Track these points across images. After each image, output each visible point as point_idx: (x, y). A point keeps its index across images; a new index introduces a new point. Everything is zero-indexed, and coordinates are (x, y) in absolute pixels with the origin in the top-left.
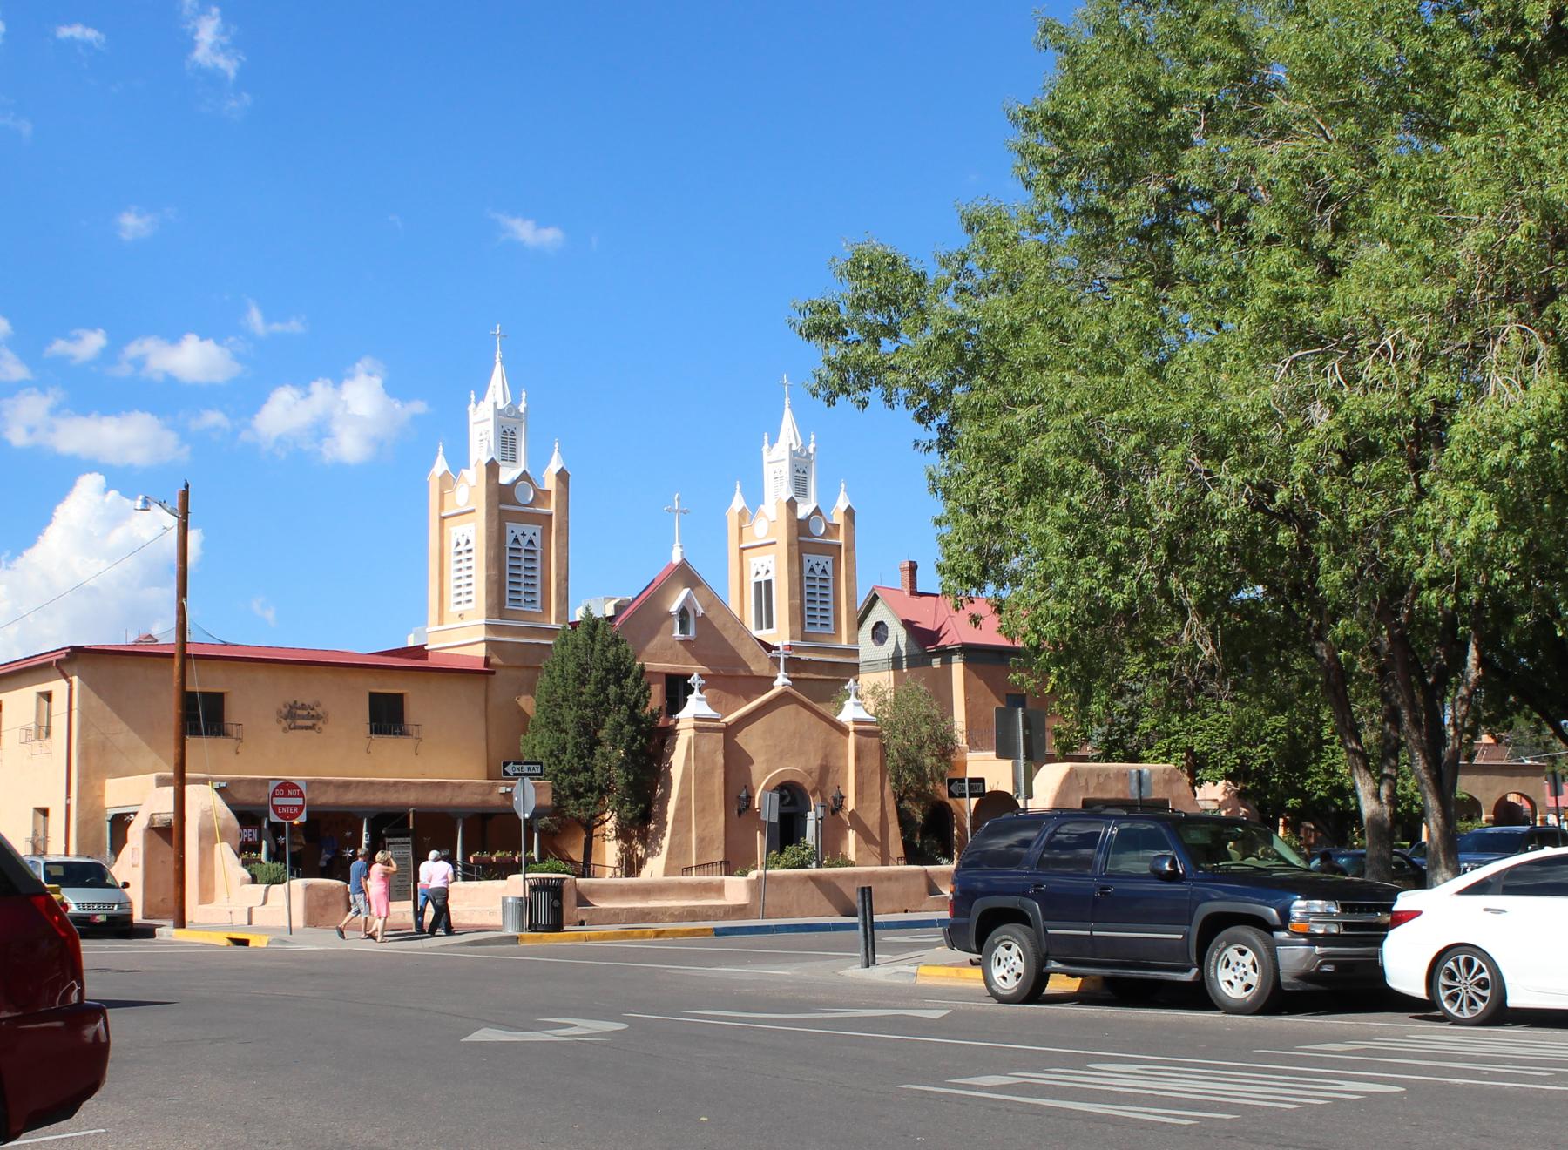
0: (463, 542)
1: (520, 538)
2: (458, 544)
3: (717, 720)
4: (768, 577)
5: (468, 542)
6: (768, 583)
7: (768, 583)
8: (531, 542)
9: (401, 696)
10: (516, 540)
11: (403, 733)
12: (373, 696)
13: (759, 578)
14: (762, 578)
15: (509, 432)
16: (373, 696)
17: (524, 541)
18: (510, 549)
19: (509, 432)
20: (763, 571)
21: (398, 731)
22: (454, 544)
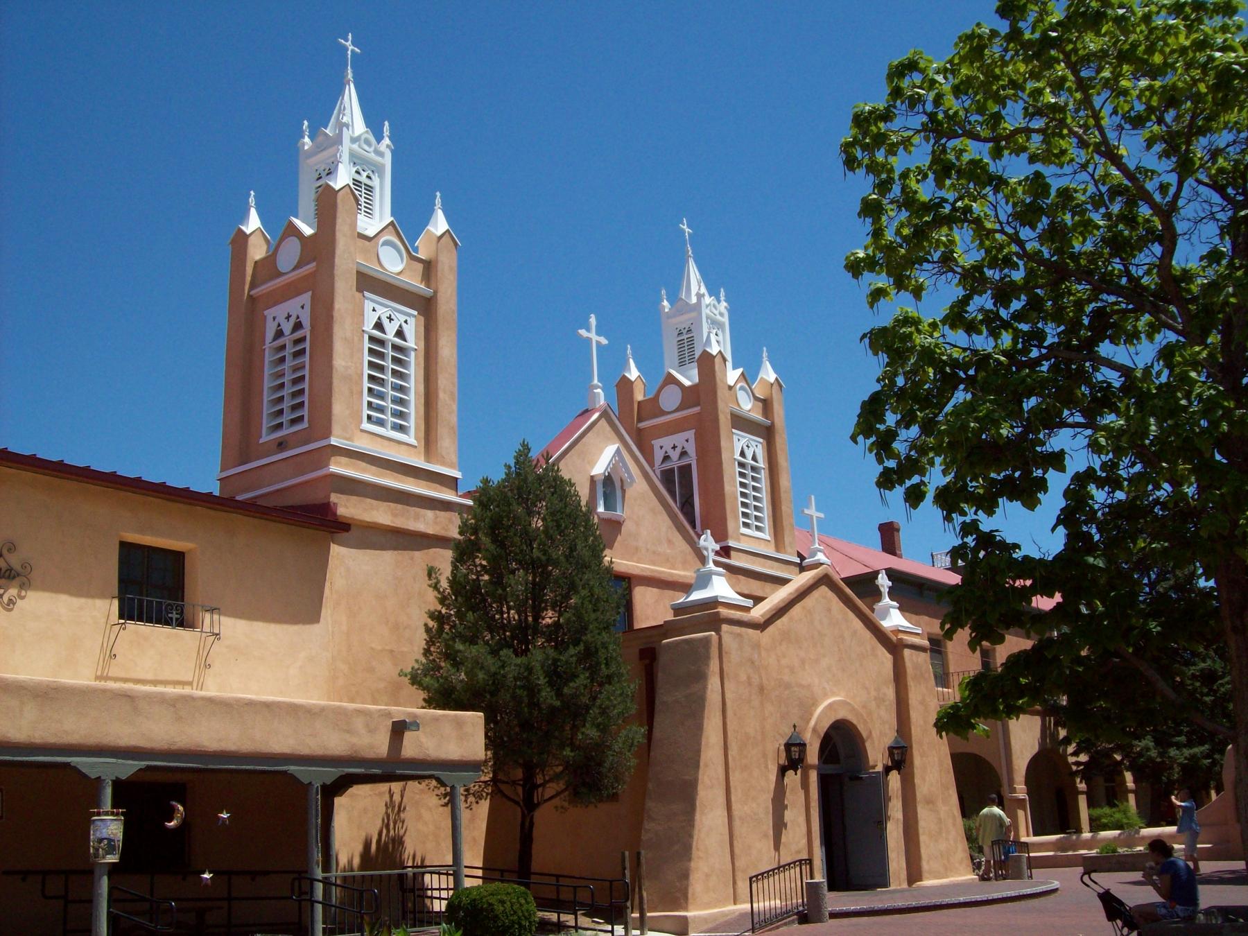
0: (287, 327)
1: (385, 322)
2: (279, 334)
3: (747, 609)
4: (684, 462)
5: (298, 326)
6: (685, 470)
7: (685, 470)
8: (400, 334)
9: (178, 558)
10: (379, 326)
11: (183, 623)
12: (128, 550)
13: (668, 465)
14: (675, 463)
16: (128, 550)
17: (391, 329)
18: (372, 339)
20: (675, 455)
21: (174, 616)
22: (270, 334)
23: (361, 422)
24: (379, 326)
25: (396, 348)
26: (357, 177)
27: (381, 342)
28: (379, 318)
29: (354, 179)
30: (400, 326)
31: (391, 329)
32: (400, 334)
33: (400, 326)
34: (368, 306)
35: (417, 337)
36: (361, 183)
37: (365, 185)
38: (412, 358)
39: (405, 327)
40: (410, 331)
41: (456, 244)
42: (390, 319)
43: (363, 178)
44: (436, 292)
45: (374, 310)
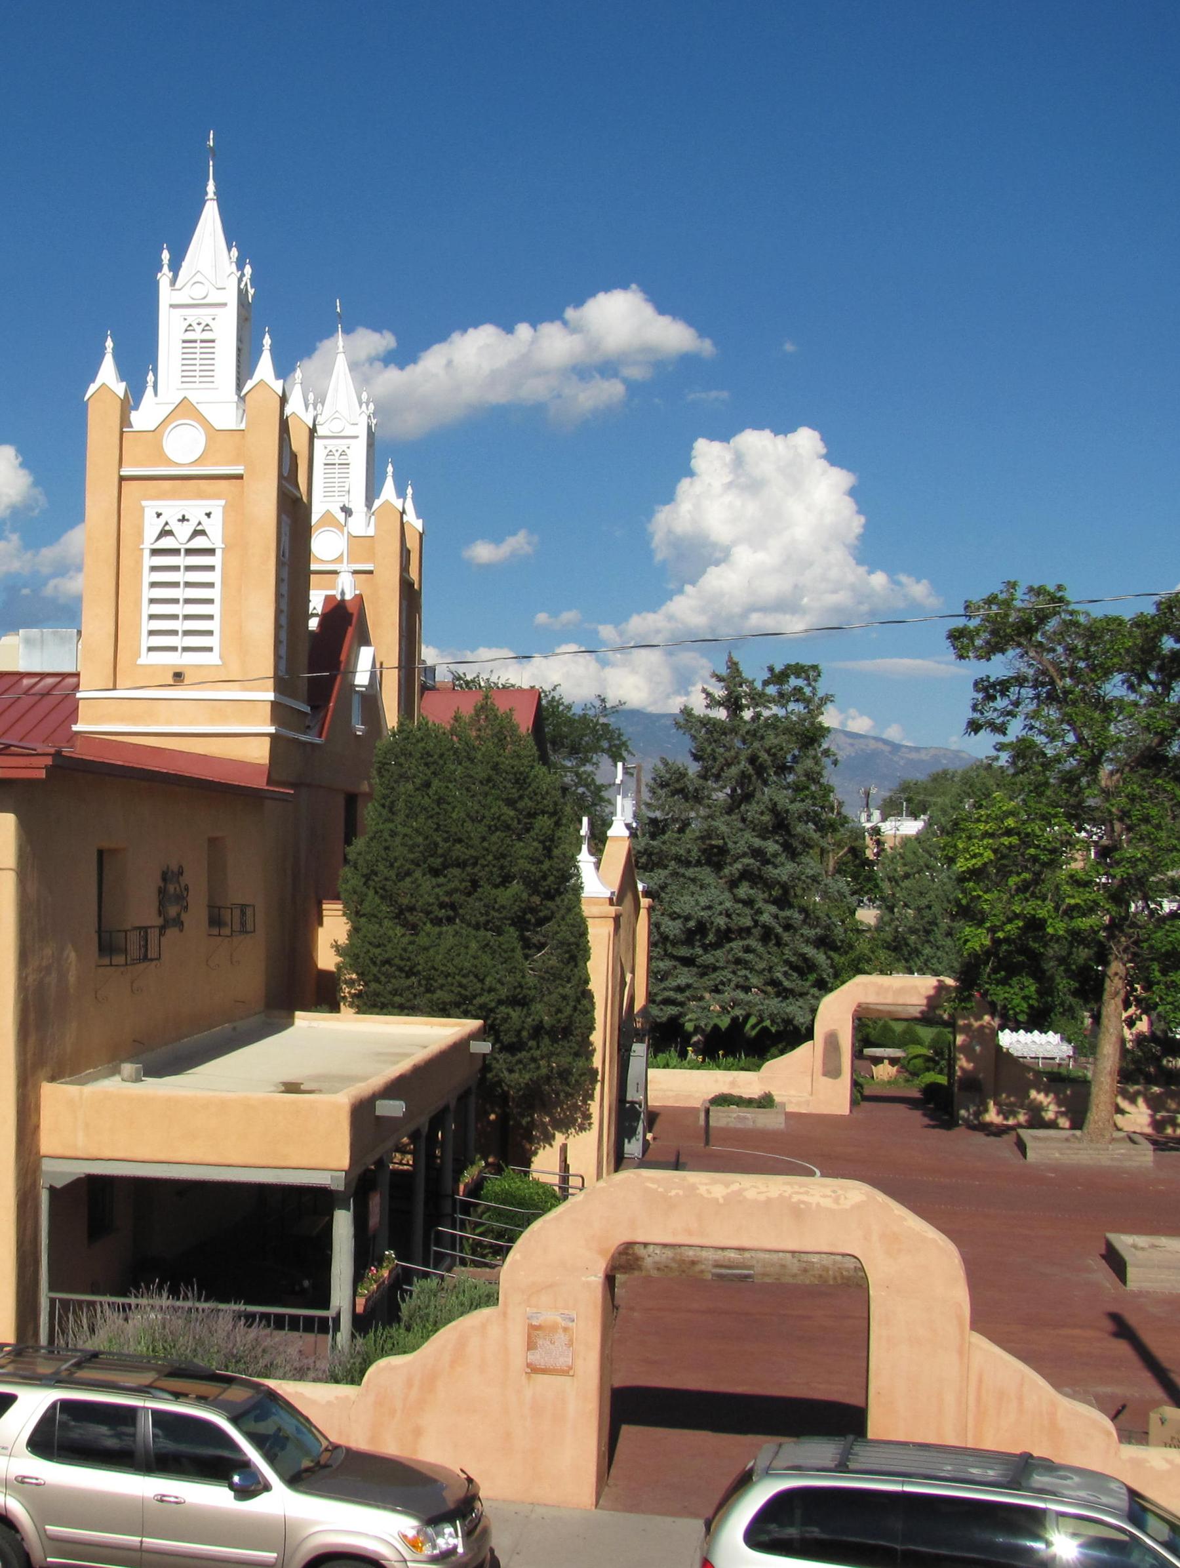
1: (174, 526)
8: (198, 533)
10: (165, 533)
18: (155, 552)
25: (189, 552)
26: (190, 336)
27: (175, 552)
28: (167, 524)
29: (184, 342)
31: (183, 532)
33: (200, 523)
34: (149, 514)
36: (195, 341)
37: (202, 341)
39: (207, 525)
43: (197, 335)
45: (159, 515)
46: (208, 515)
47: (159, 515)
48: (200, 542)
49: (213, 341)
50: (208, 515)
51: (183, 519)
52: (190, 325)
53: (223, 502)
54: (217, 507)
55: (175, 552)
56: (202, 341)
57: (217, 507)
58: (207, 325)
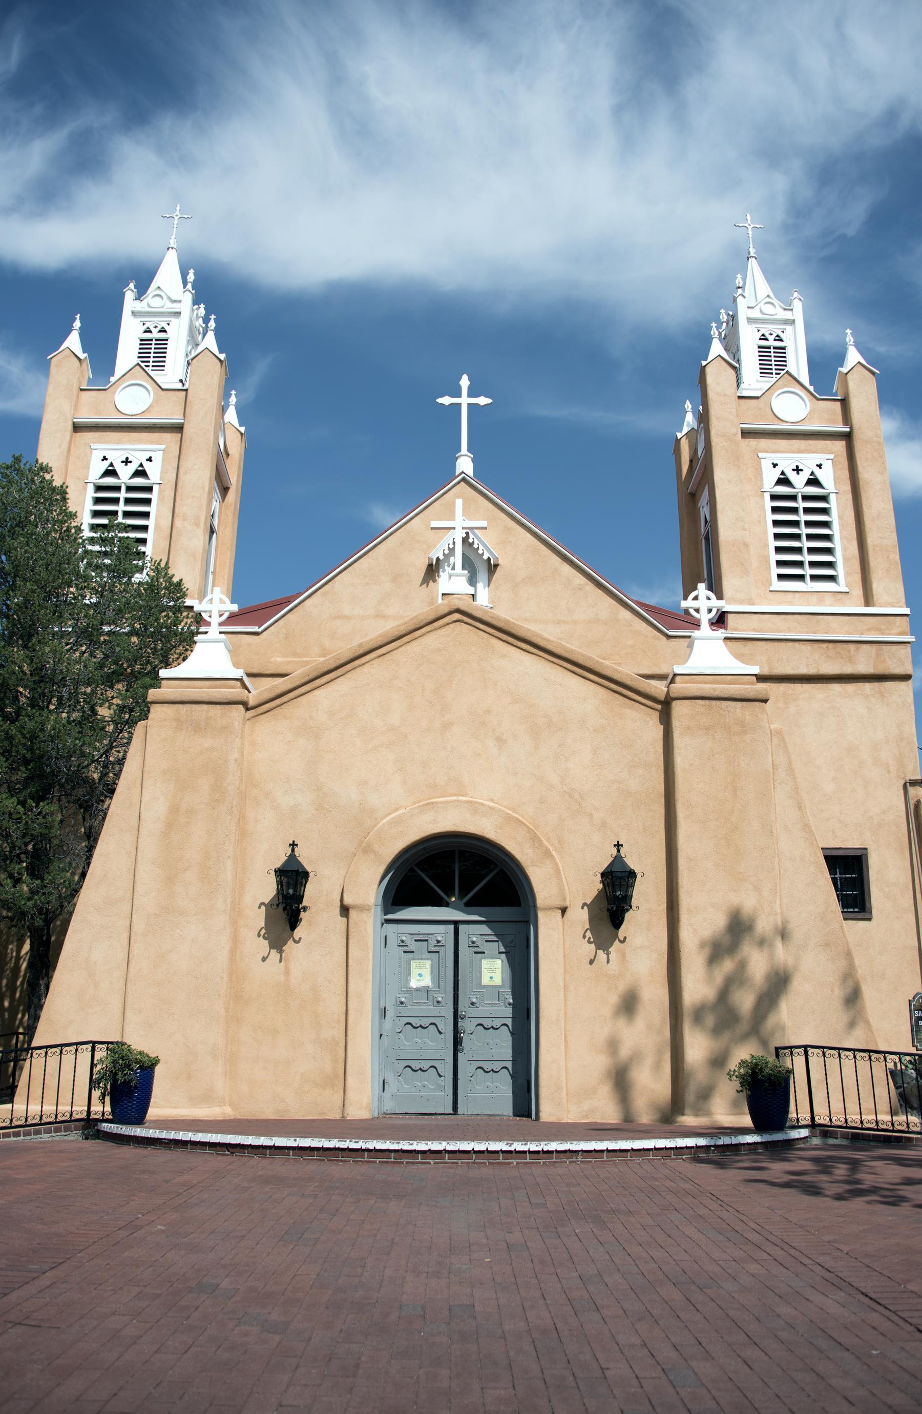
1: (792, 476)
10: (783, 481)
15: (771, 338)
17: (798, 481)
18: (774, 497)
19: (771, 338)
23: (771, 585)
24: (783, 481)
25: (806, 498)
27: (793, 498)
28: (783, 473)
30: (812, 473)
32: (813, 481)
34: (766, 465)
35: (836, 480)
36: (769, 348)
37: (774, 348)
38: (833, 503)
39: (820, 475)
40: (826, 476)
41: (873, 373)
42: (798, 470)
43: (771, 342)
44: (851, 428)
45: (775, 465)
46: (820, 466)
47: (775, 465)
48: (813, 490)
49: (784, 348)
50: (820, 466)
51: (798, 470)
52: (763, 335)
53: (832, 456)
54: (826, 459)
55: (793, 498)
56: (774, 348)
57: (826, 459)
58: (778, 336)
